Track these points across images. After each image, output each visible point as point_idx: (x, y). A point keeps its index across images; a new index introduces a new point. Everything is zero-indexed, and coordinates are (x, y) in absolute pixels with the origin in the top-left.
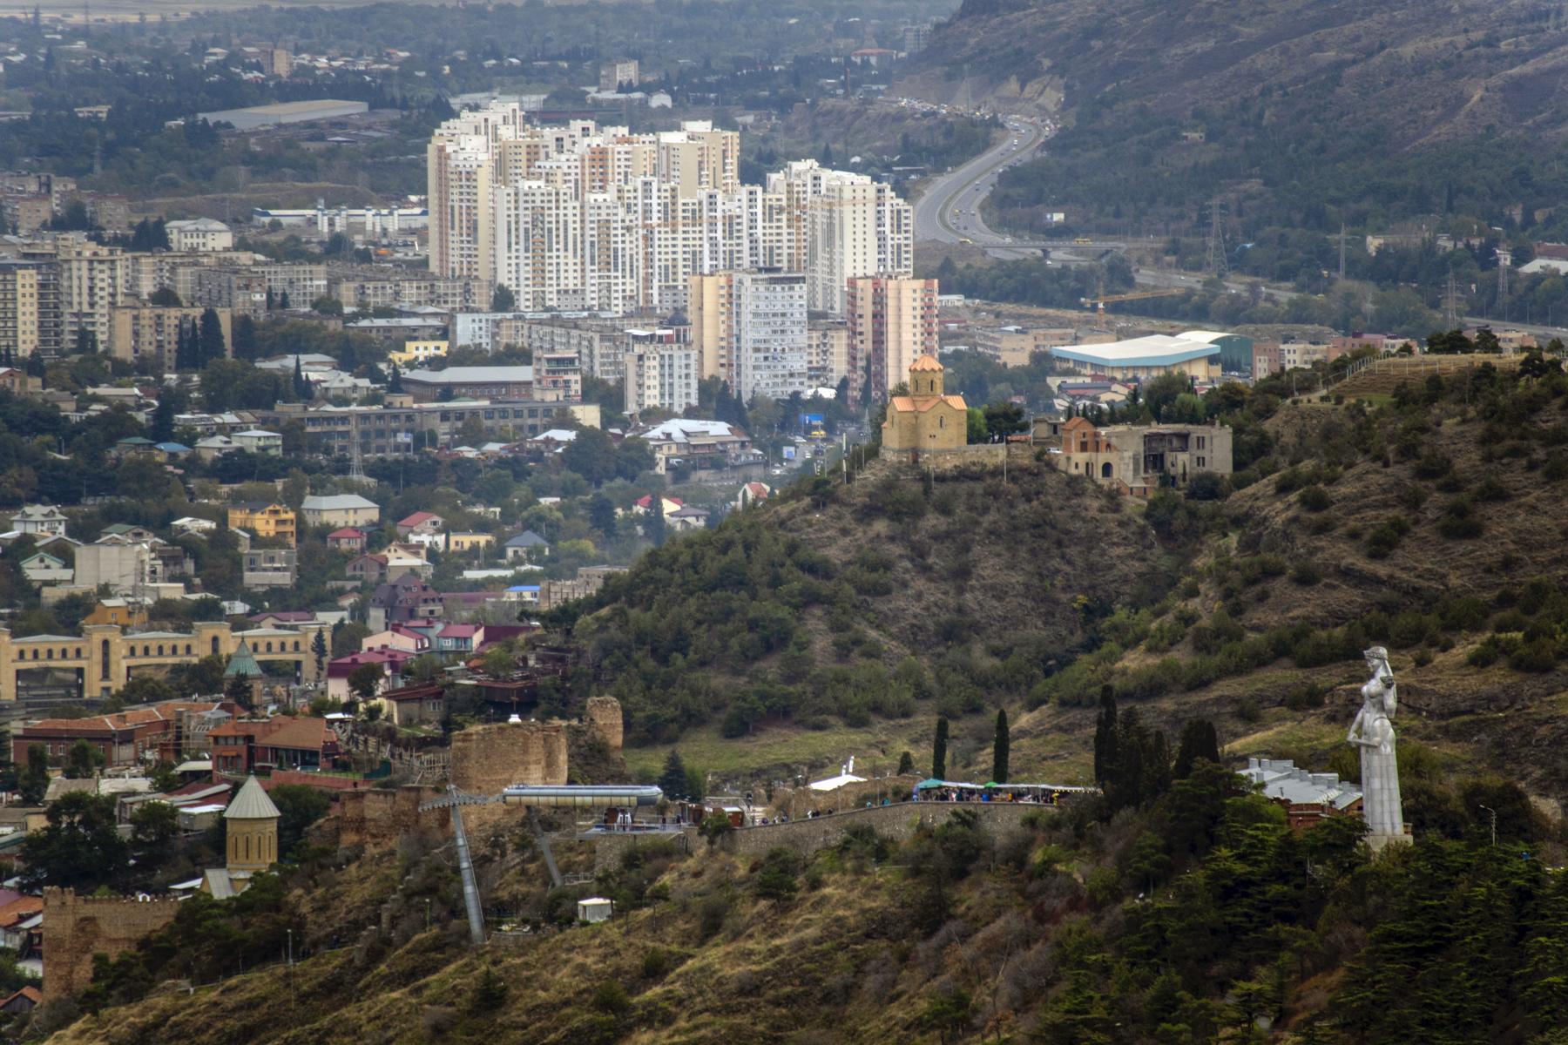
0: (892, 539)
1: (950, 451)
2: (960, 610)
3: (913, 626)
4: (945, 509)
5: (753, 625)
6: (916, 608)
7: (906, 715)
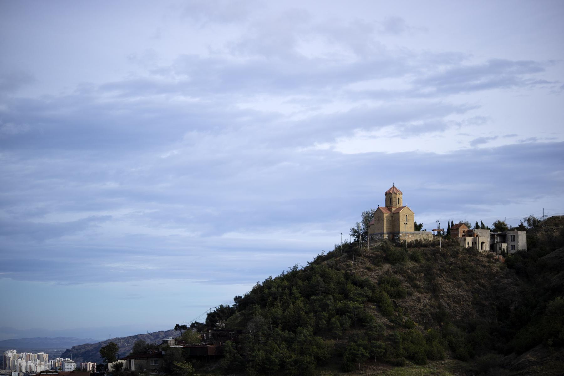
0: (395, 272)
1: (410, 233)
2: (440, 307)
3: (421, 315)
4: (414, 258)
6: (421, 306)
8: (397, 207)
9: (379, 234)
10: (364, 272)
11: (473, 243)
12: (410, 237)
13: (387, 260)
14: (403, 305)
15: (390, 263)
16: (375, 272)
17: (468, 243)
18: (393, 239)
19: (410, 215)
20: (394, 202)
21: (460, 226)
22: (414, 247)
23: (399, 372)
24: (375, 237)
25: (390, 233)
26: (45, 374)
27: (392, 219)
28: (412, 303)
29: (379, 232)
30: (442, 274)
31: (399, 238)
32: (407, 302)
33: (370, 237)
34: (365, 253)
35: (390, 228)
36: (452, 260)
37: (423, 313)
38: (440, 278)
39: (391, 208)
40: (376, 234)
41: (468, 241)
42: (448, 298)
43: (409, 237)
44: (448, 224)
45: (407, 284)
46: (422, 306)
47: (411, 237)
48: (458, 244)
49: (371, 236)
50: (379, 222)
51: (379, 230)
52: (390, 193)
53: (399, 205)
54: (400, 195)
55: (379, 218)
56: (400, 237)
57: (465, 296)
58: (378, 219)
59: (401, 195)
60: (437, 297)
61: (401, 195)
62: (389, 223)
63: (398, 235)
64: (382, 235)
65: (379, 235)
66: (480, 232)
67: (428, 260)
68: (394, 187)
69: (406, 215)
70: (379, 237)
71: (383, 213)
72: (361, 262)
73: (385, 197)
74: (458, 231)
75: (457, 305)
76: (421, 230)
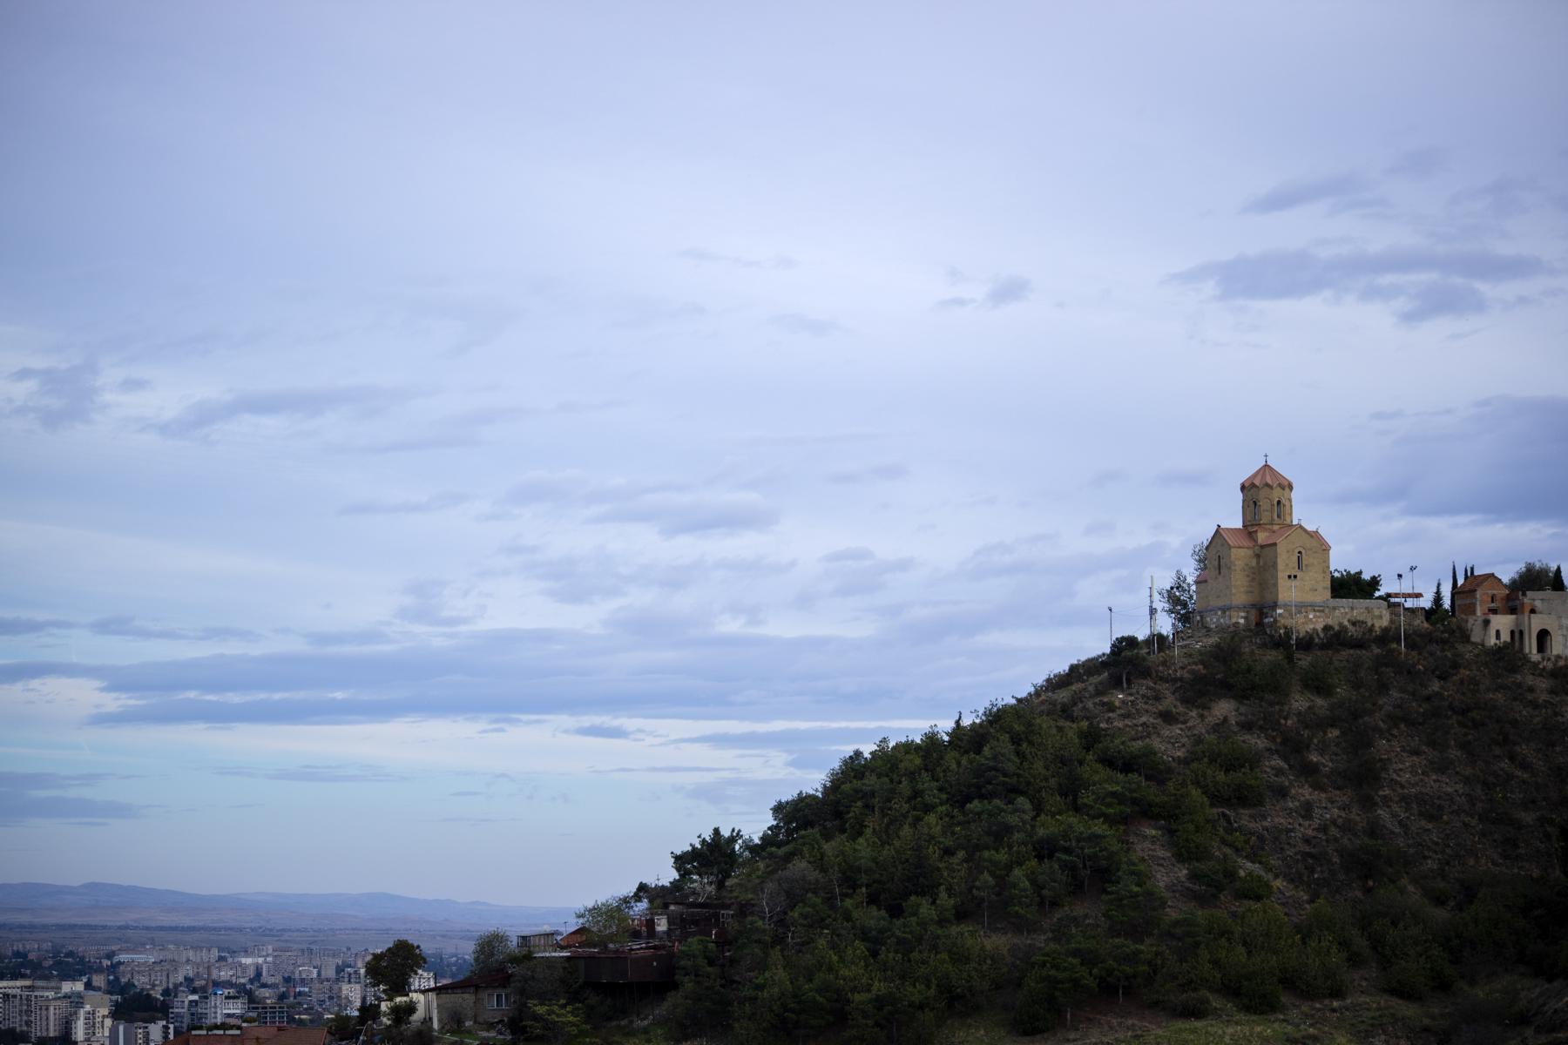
0: (1247, 726)
1: (1313, 607)
2: (1374, 830)
4: (1317, 684)
5: (1045, 850)
6: (1307, 829)
7: (1337, 993)
9: (1220, 609)
10: (1148, 727)
11: (1512, 633)
12: (1311, 616)
13: (1227, 689)
14: (1252, 825)
15: (1235, 697)
16: (1183, 726)
17: (1498, 632)
18: (1259, 624)
20: (1267, 511)
21: (1482, 583)
23: (1184, 1035)
24: (1208, 619)
25: (1252, 605)
26: (204, 1032)
27: (1258, 563)
28: (1282, 821)
29: (1220, 603)
30: (1395, 732)
31: (1276, 621)
32: (1266, 819)
33: (1198, 618)
34: (1161, 668)
35: (1251, 592)
36: (1436, 686)
37: (1312, 850)
38: (1388, 741)
39: (1256, 531)
40: (1211, 611)
41: (1497, 628)
42: (1403, 804)
43: (1306, 617)
44: (1451, 575)
45: (1278, 762)
46: (1313, 830)
47: (1314, 617)
48: (1465, 637)
49: (1202, 617)
51: (1218, 597)
52: (1253, 485)
54: (1284, 489)
55: (1219, 561)
56: (1278, 619)
57: (1458, 798)
58: (1217, 563)
59: (1287, 489)
60: (1367, 803)
61: (1287, 489)
62: (1248, 576)
64: (1227, 613)
65: (1220, 613)
66: (1542, 600)
67: (1357, 685)
68: (1269, 466)
69: (1297, 551)
70: (1218, 620)
72: (1143, 696)
73: (1240, 496)
75: (1430, 826)
76: (1377, 594)
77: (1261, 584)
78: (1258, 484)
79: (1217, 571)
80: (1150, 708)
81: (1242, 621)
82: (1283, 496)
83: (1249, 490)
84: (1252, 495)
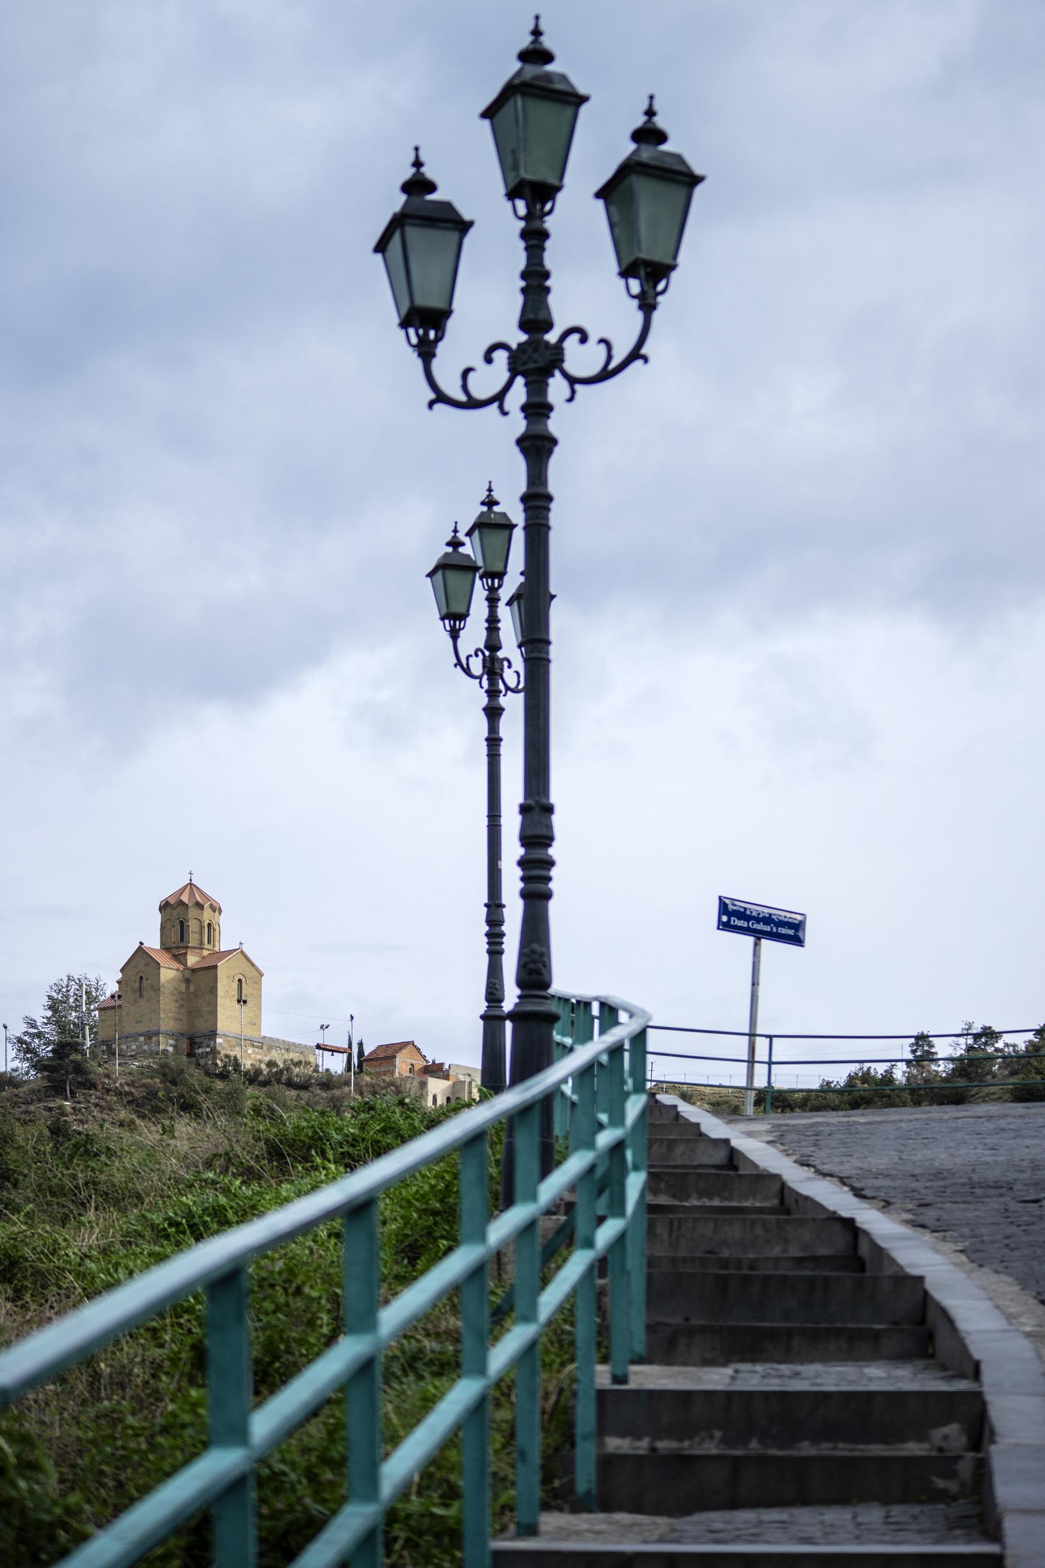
8: (205, 953)
12: (250, 1051)
17: (435, 1097)
18: (190, 1055)
19: (251, 979)
21: (400, 1049)
22: (265, 1084)
27: (188, 988)
29: (141, 1028)
39: (186, 954)
40: (127, 1037)
47: (254, 1052)
50: (141, 996)
52: (181, 903)
53: (210, 947)
54: (214, 912)
58: (137, 984)
61: (217, 911)
62: (177, 1001)
63: (212, 1043)
64: (154, 1039)
70: (140, 1046)
71: (158, 964)
73: (157, 918)
74: (394, 1066)
77: (189, 1012)
78: (187, 902)
79: (138, 994)
80: (106, 1117)
81: (171, 1049)
82: (214, 918)
83: (174, 909)
84: (178, 914)
